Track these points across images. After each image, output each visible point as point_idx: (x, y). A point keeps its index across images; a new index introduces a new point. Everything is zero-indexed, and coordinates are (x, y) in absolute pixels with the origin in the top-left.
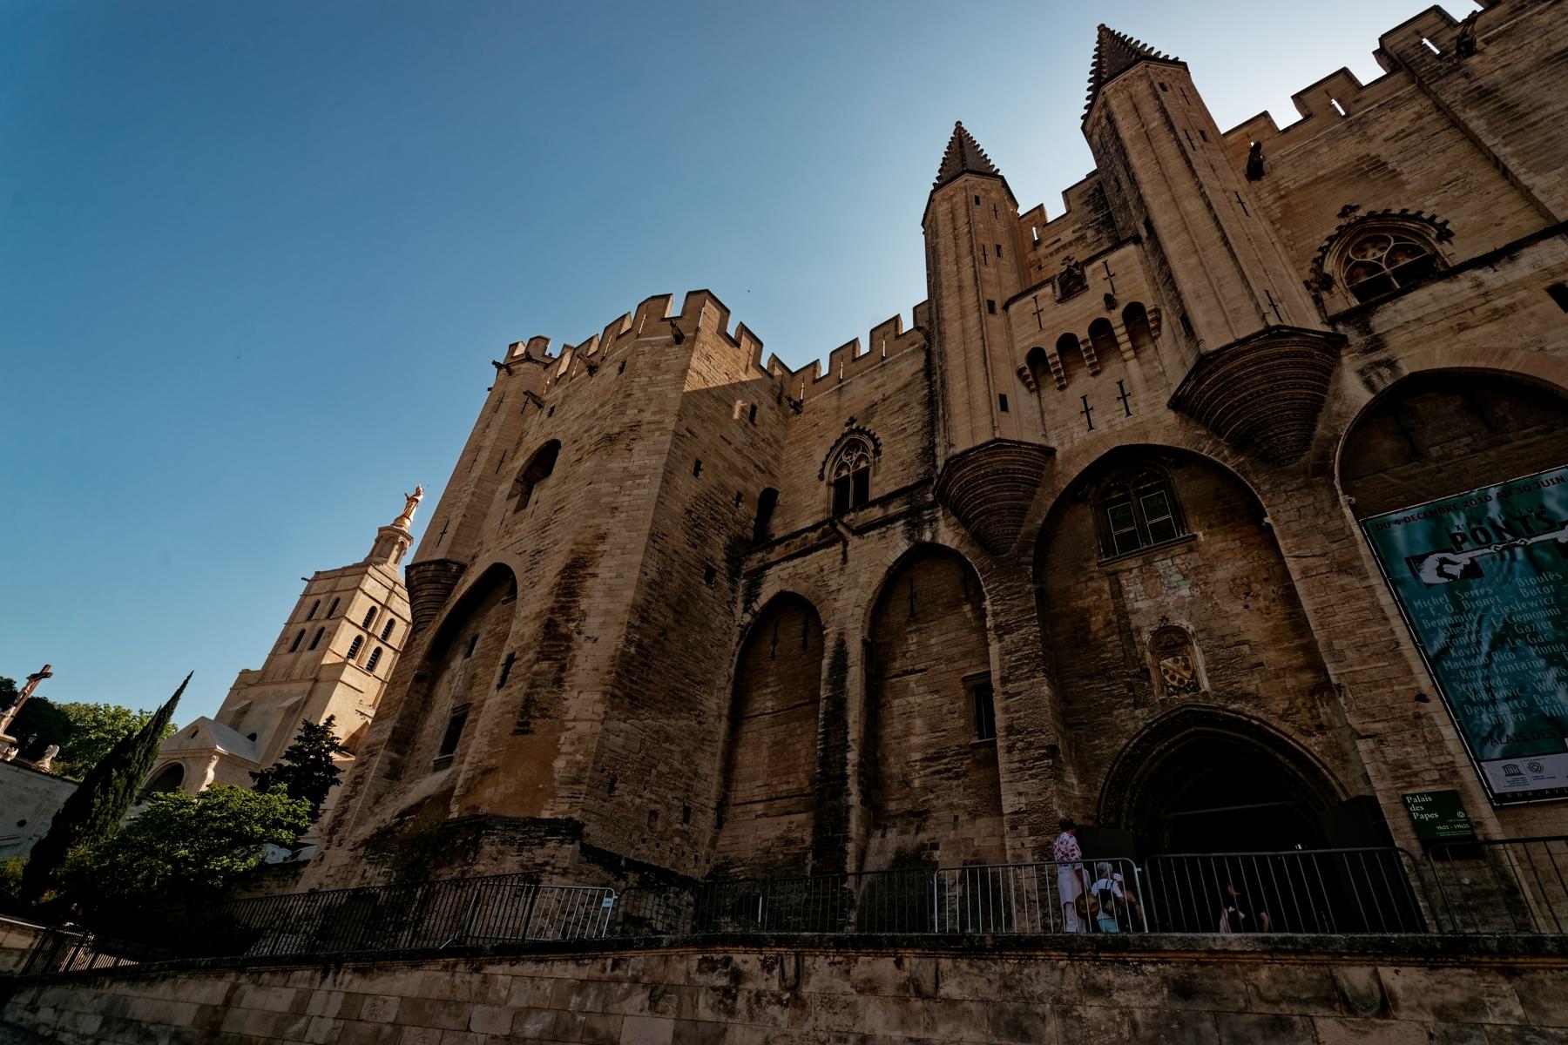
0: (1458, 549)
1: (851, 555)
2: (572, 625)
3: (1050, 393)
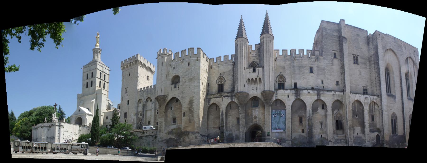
0: (276, 115)
1: (223, 100)
3: (249, 85)
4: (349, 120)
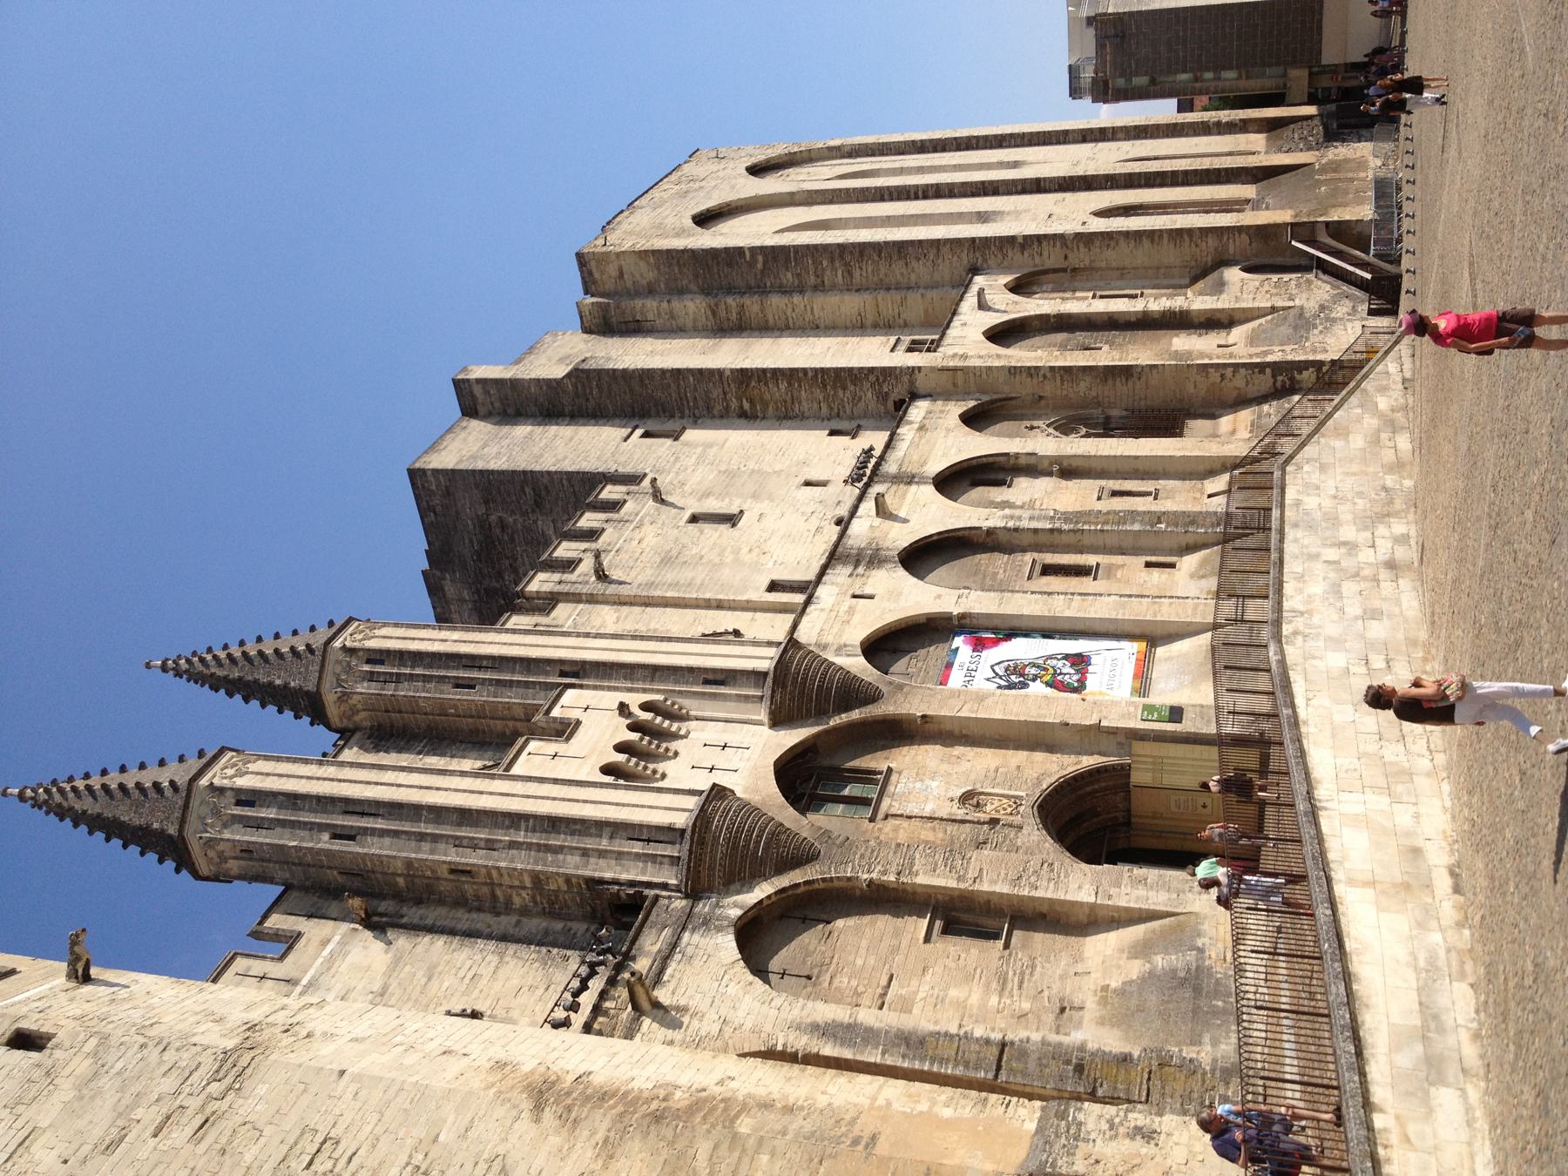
1: (682, 1002)
2: (678, 1094)
4: (1120, 360)
